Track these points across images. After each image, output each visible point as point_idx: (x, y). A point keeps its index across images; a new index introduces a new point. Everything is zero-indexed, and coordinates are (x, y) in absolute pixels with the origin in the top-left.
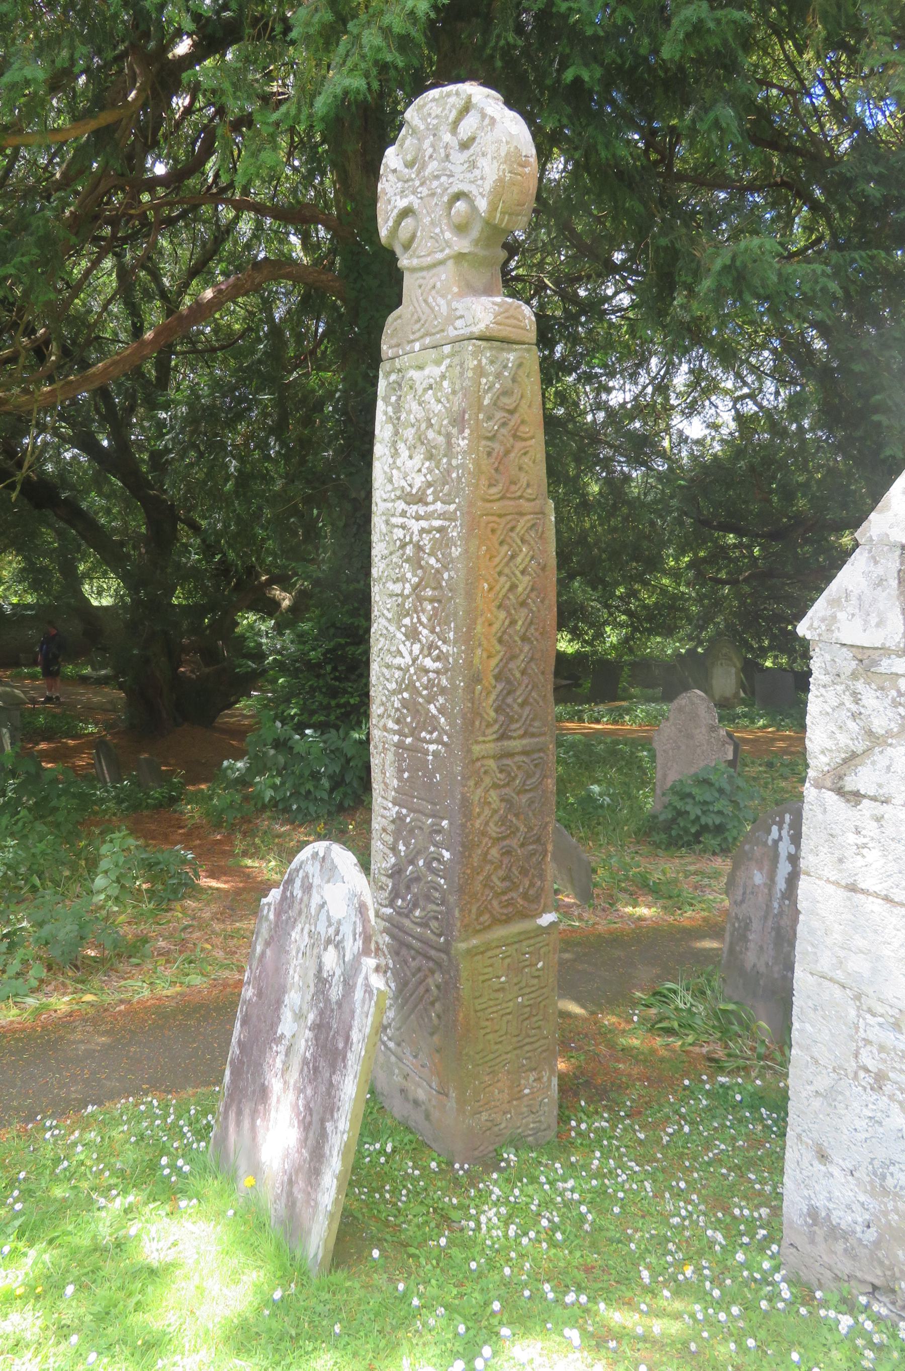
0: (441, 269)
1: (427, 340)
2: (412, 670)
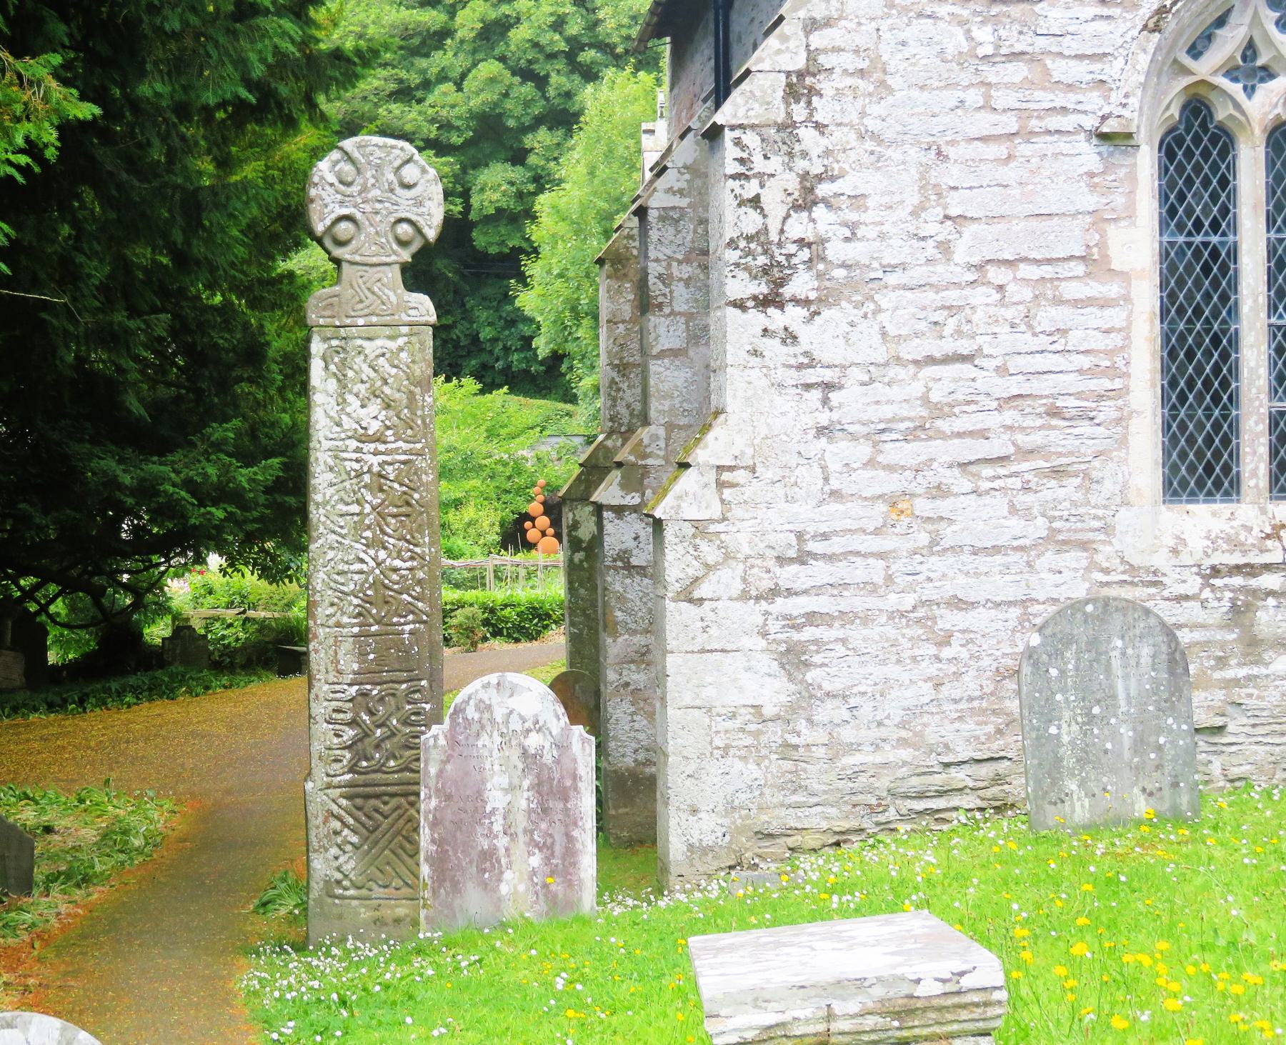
0: (386, 268)
2: (377, 571)
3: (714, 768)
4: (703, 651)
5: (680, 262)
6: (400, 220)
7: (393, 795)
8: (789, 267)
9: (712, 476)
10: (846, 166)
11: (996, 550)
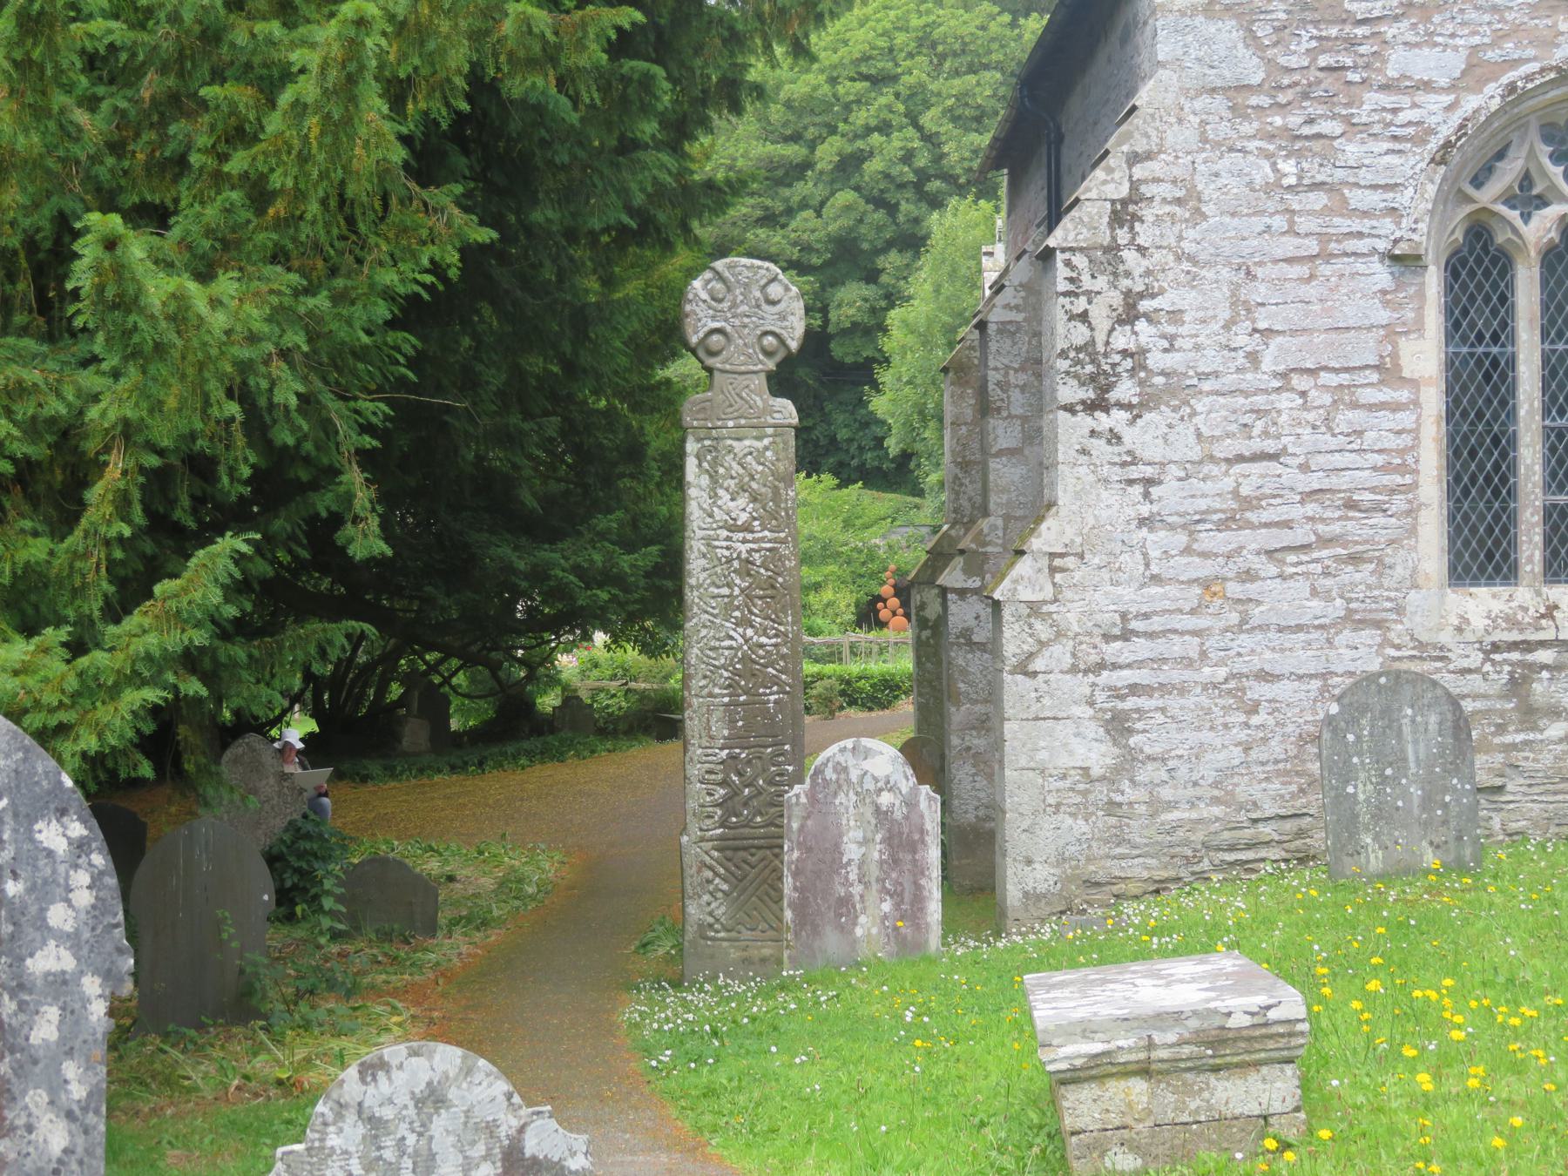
1: (743, 422)
3: (1048, 823)
4: (1037, 719)
5: (1016, 371)
6: (766, 333)
7: (759, 848)
8: (1115, 375)
9: (1045, 562)
10: (1165, 285)
11: (1299, 628)
